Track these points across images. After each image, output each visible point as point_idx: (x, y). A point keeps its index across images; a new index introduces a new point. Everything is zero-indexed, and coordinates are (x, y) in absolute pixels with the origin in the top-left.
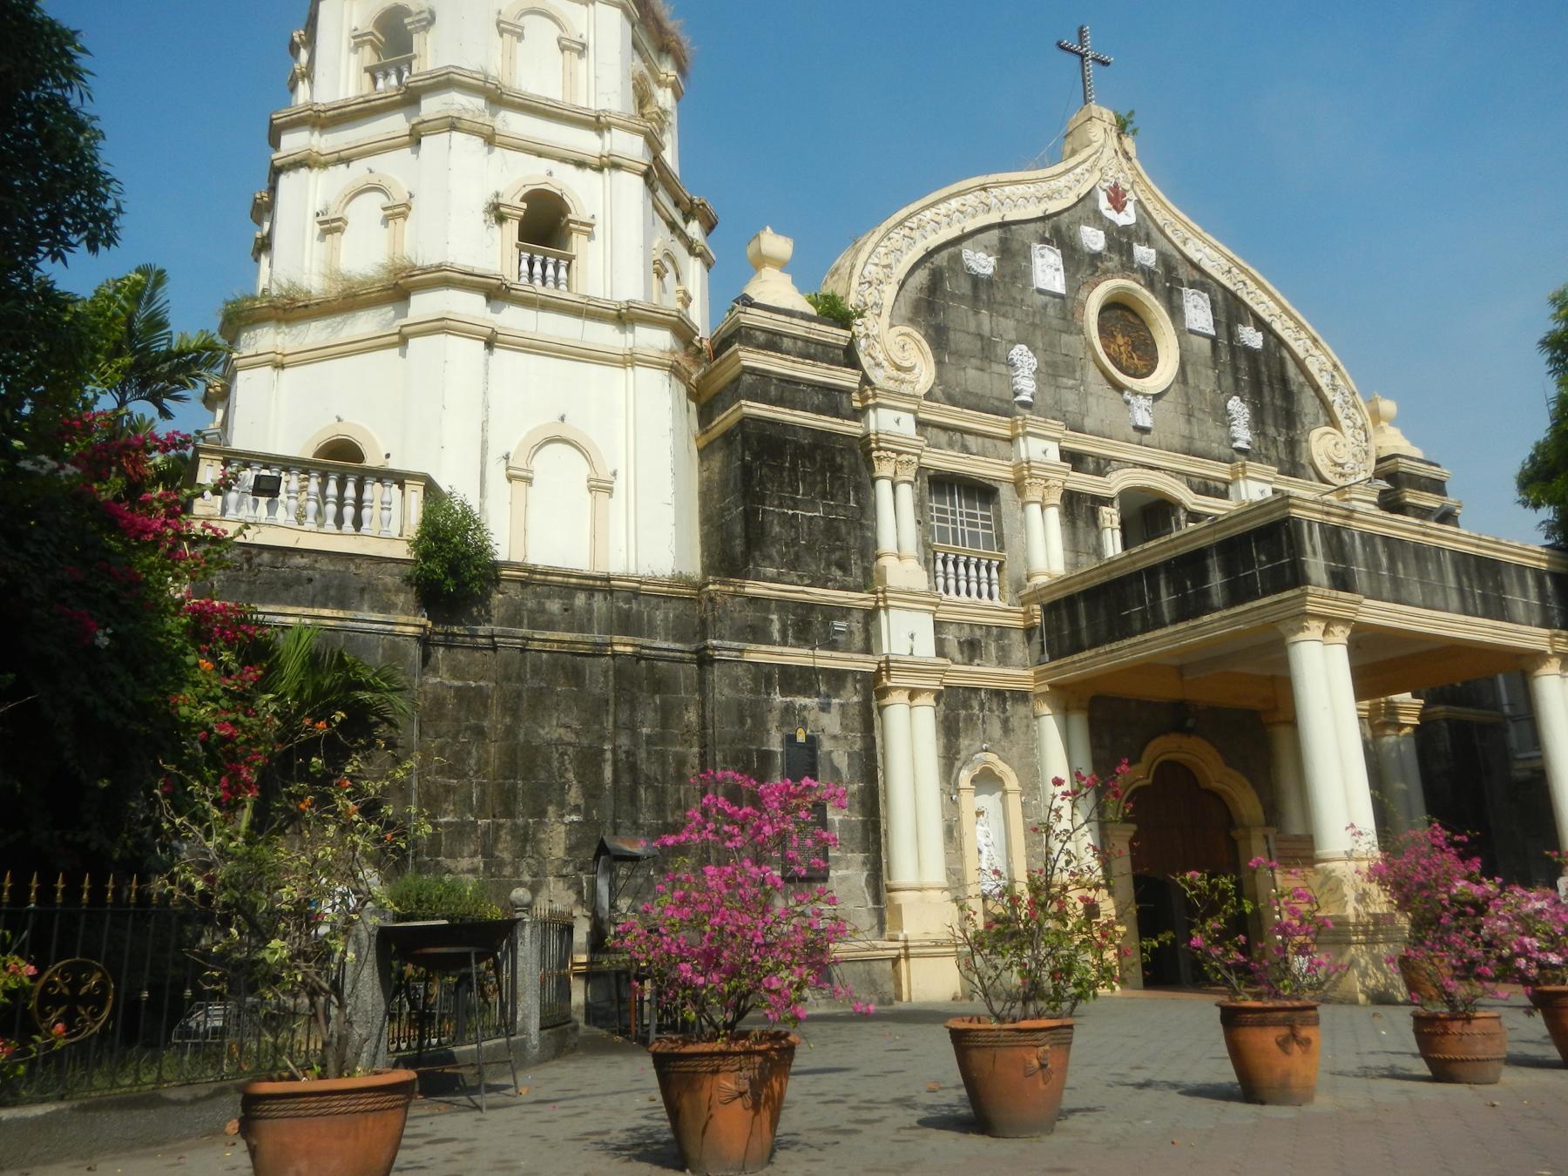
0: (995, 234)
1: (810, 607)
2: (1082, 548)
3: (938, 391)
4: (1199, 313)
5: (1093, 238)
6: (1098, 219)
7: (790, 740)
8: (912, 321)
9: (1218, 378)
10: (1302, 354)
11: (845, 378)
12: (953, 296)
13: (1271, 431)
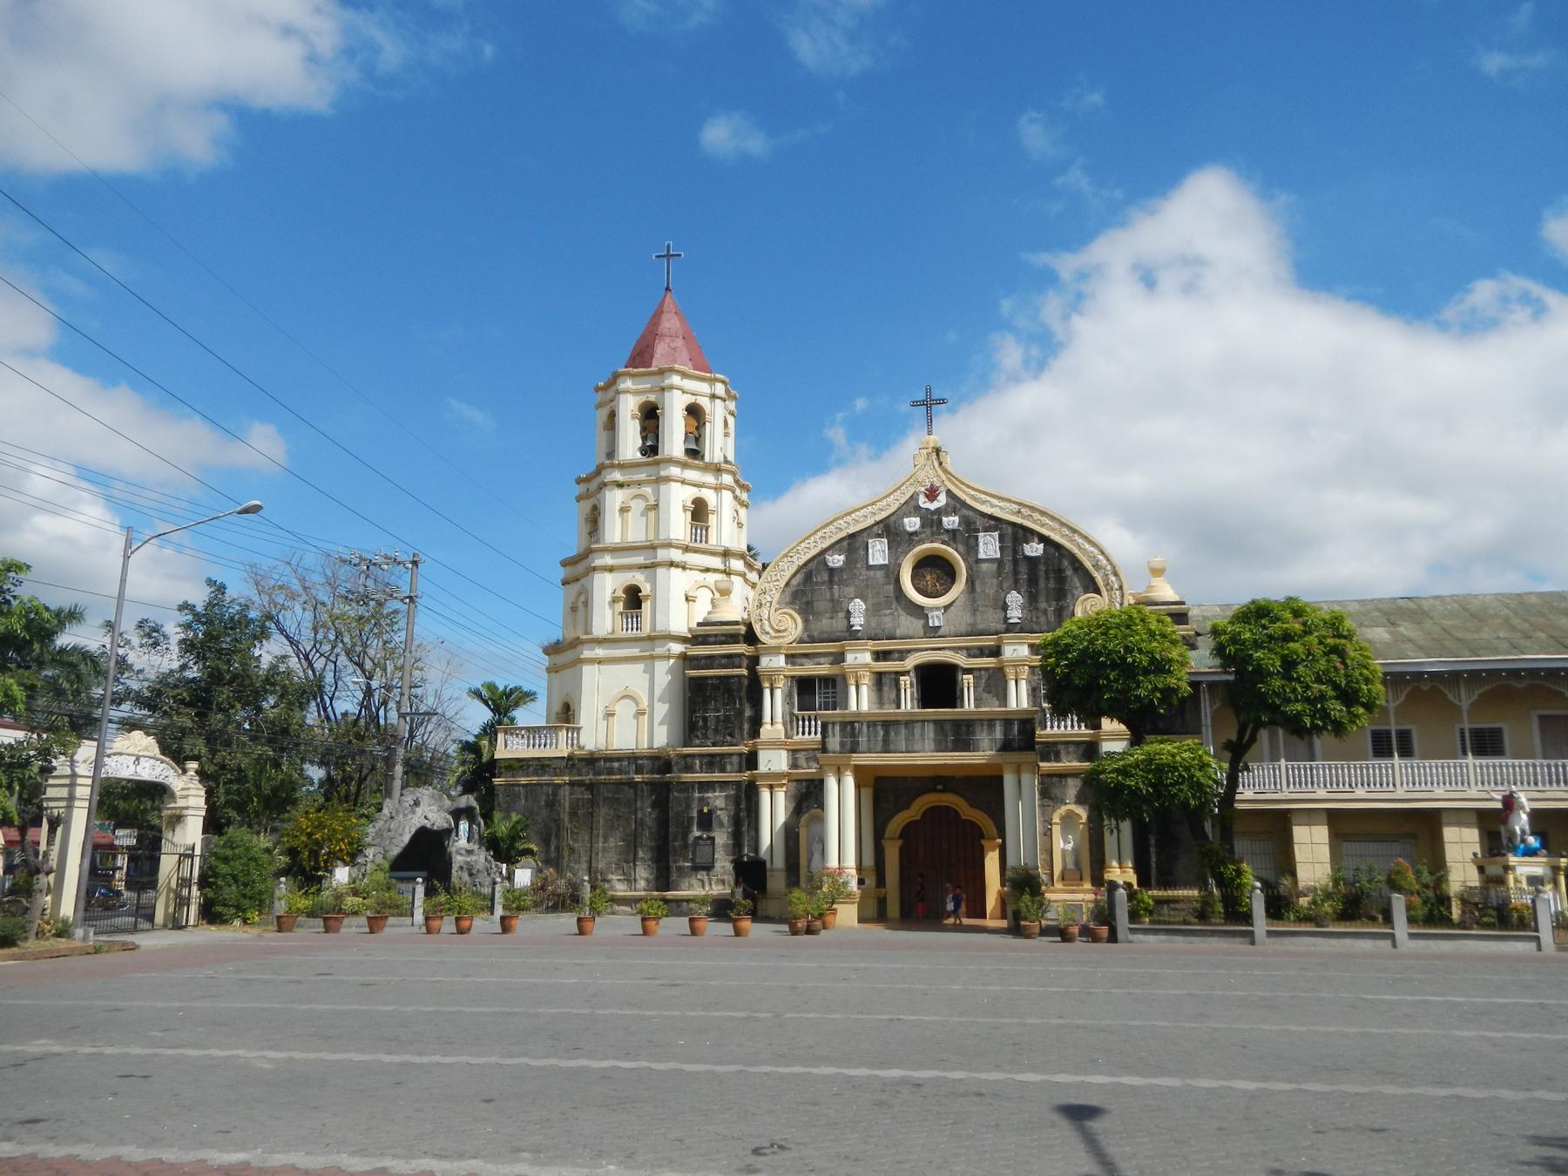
0: (845, 543)
1: (713, 756)
2: (886, 700)
3: (805, 637)
4: (989, 546)
5: (912, 523)
6: (918, 508)
7: (700, 812)
8: (791, 603)
9: (1000, 585)
10: (1076, 551)
11: (741, 648)
12: (817, 583)
13: (1043, 605)
